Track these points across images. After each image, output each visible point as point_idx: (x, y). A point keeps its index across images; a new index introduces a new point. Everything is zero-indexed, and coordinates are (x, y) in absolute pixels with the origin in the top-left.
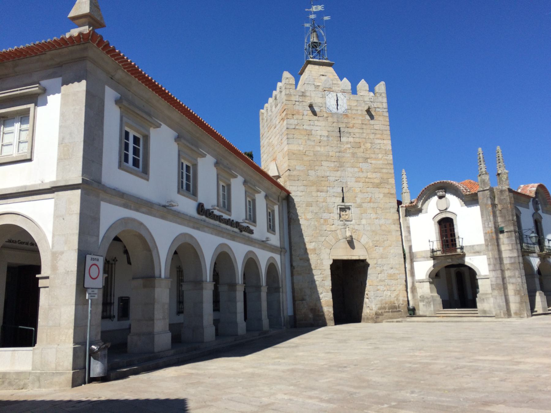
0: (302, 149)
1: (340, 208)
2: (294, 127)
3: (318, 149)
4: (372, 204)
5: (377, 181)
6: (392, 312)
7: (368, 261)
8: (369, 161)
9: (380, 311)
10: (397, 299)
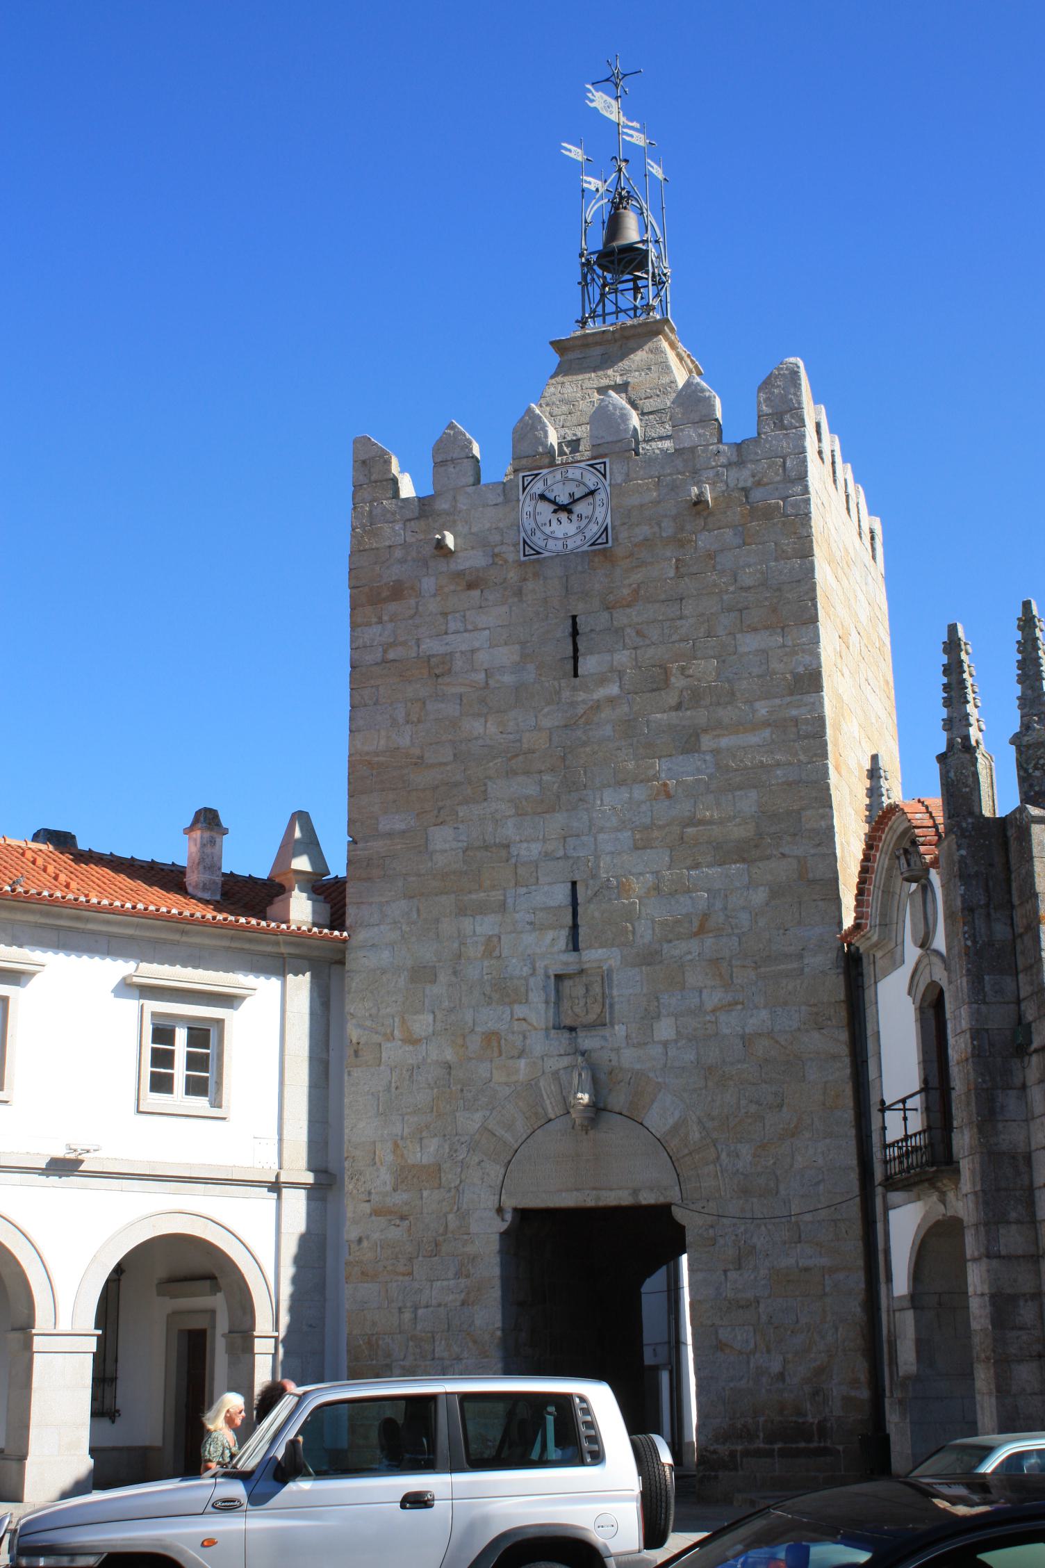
0: (405, 741)
1: (559, 978)
2: (378, 656)
3: (475, 727)
4: (709, 941)
5: (738, 832)
6: (783, 1453)
7: (679, 1214)
8: (707, 742)
9: (723, 1449)
10: (816, 1393)
